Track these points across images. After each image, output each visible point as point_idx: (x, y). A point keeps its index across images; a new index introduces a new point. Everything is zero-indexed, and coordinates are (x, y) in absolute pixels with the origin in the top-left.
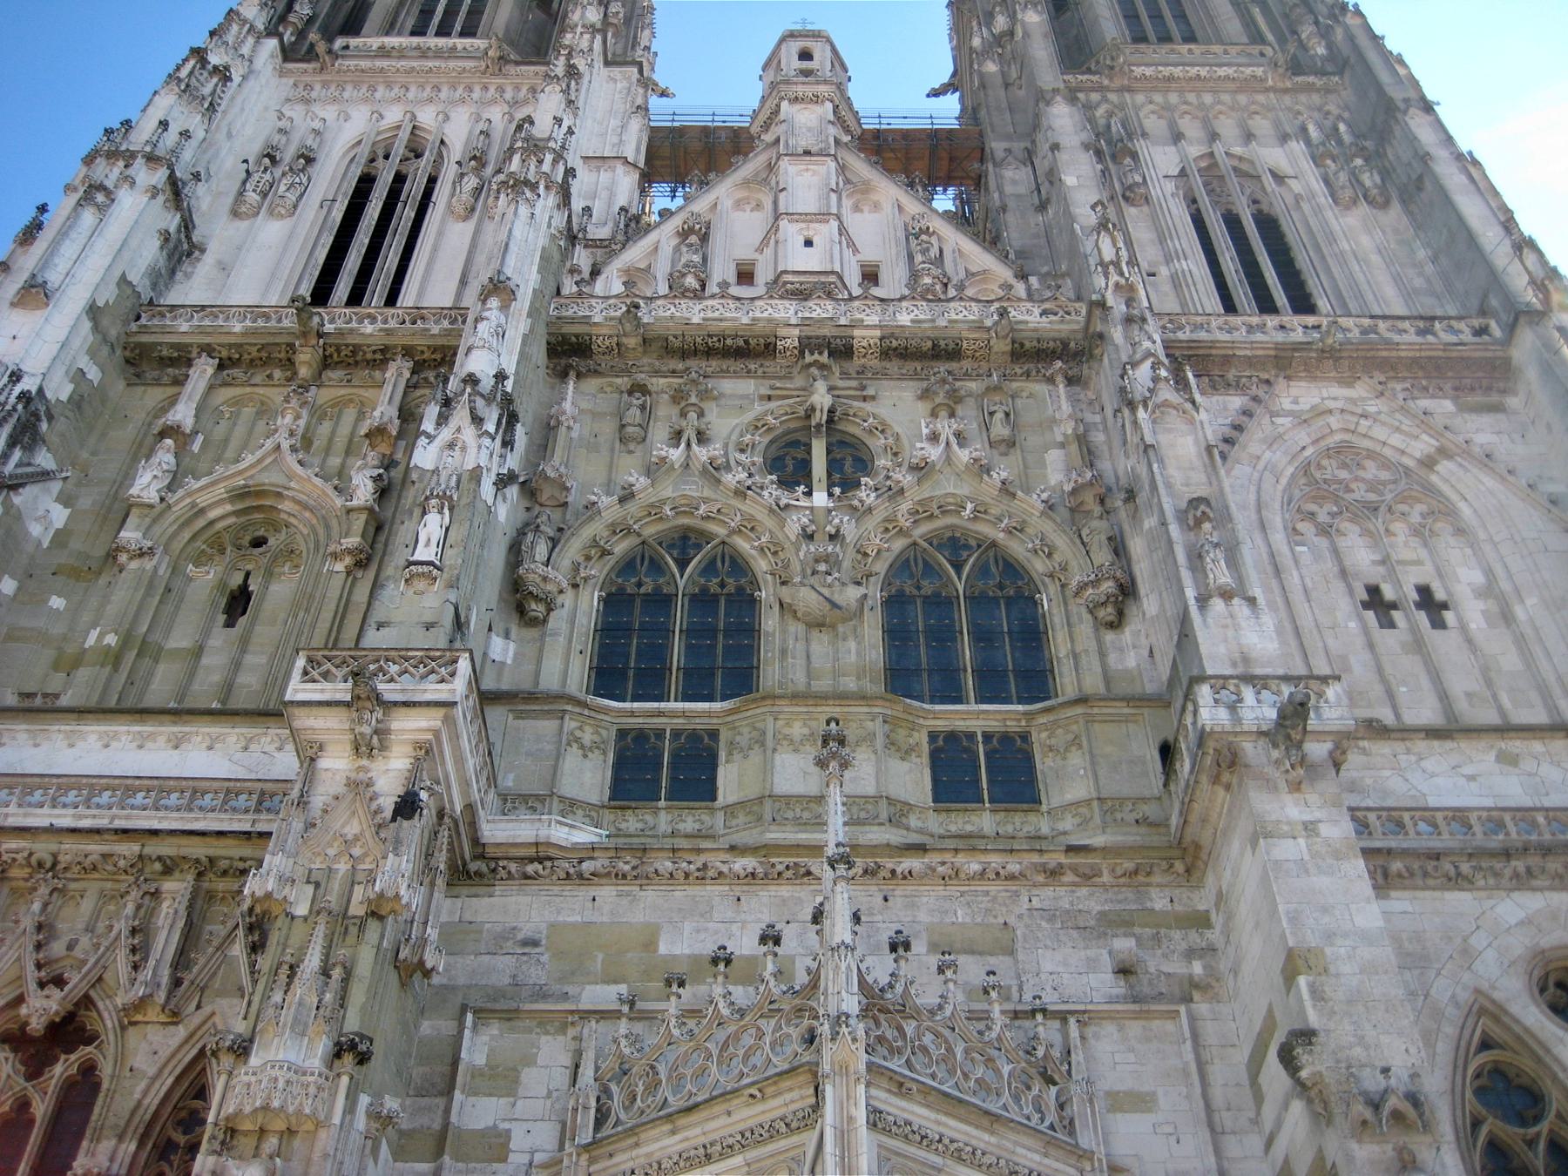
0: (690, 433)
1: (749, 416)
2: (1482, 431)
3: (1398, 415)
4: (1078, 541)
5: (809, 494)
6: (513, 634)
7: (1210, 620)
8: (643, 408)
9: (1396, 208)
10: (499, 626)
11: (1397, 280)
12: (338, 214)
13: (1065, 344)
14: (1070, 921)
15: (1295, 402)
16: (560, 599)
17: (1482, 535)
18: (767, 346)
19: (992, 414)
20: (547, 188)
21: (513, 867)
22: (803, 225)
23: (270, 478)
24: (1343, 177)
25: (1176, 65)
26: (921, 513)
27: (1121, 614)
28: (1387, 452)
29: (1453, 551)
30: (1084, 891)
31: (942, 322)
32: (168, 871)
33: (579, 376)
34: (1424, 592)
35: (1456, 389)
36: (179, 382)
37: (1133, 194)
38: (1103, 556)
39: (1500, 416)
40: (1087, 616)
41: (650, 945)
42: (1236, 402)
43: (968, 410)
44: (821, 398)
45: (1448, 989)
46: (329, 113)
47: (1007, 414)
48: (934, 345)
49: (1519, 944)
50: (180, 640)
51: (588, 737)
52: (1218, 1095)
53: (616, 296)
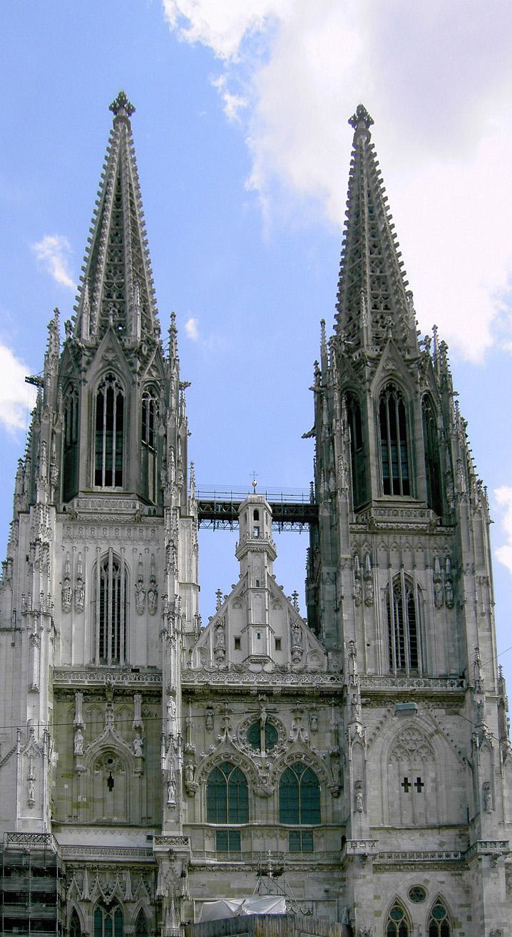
2: (449, 724)
3: (428, 717)
9: (455, 610)
12: (98, 612)
13: (336, 692)
14: (317, 880)
19: (312, 719)
21: (198, 869)
23: (110, 742)
24: (441, 594)
25: (394, 523)
27: (339, 794)
28: (421, 730)
29: (430, 764)
30: (320, 873)
32: (123, 869)
34: (419, 779)
35: (448, 705)
36: (73, 700)
37: (368, 603)
39: (457, 717)
41: (229, 885)
42: (383, 711)
44: (264, 716)
45: (391, 895)
46: (79, 546)
50: (99, 796)
51: (210, 834)
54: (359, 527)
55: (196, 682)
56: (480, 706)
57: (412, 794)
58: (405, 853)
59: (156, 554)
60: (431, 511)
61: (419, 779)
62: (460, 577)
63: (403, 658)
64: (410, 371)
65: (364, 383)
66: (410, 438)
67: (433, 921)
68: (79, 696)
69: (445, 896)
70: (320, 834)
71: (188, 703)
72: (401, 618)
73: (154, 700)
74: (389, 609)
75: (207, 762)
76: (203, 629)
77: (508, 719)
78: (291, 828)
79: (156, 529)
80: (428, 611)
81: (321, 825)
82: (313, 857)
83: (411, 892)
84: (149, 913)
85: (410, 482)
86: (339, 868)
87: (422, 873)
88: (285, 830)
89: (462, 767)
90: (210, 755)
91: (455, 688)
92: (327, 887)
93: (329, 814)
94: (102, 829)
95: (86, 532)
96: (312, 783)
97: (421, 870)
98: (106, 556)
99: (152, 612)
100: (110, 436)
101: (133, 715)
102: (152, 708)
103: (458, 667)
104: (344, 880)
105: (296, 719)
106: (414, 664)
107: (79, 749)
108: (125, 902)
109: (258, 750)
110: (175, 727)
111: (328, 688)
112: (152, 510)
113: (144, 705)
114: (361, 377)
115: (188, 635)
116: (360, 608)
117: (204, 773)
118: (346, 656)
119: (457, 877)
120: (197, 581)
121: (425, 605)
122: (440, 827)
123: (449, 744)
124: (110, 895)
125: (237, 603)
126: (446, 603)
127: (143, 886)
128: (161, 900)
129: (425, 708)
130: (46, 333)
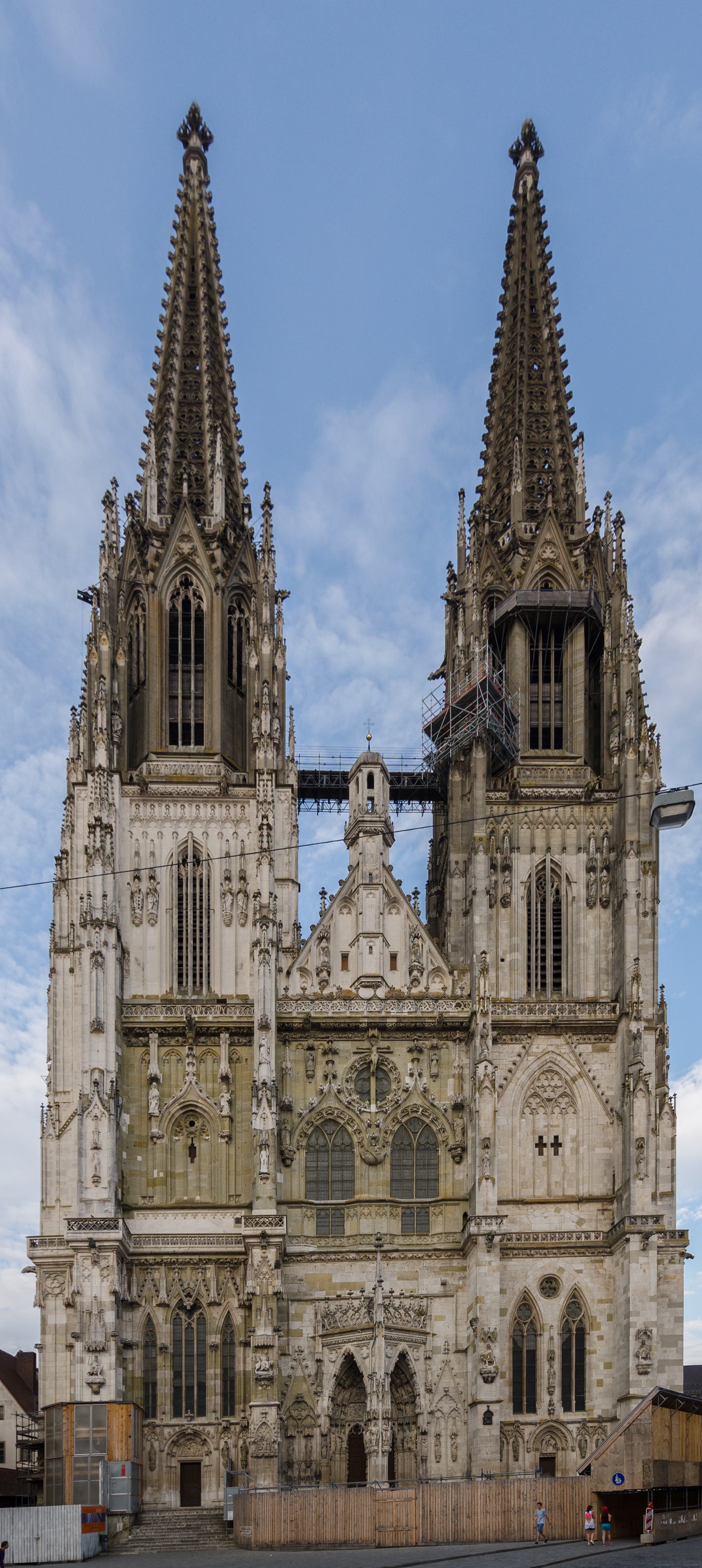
1: (349, 1063)
3: (571, 1055)
8: (313, 1060)
11: (597, 963)
15: (537, 1048)
17: (581, 1115)
21: (294, 1258)
23: (191, 1097)
26: (405, 1112)
27: (461, 1158)
32: (206, 1263)
33: (289, 1042)
36: (146, 1045)
37: (506, 902)
39: (605, 1054)
40: (451, 1160)
41: (330, 1280)
42: (518, 1048)
43: (424, 1057)
45: (518, 1287)
46: (153, 831)
49: (539, 1274)
51: (309, 1213)
52: (459, 1318)
54: (498, 794)
55: (296, 1012)
56: (636, 1037)
57: (548, 1157)
58: (537, 1233)
59: (247, 842)
60: (589, 769)
61: (556, 1138)
62: (620, 862)
63: (543, 977)
64: (573, 559)
65: (512, 581)
66: (567, 663)
67: (567, 1321)
68: (154, 1036)
69: (583, 1289)
70: (437, 1210)
71: (284, 1043)
72: (543, 923)
73: (244, 1040)
74: (529, 910)
75: (306, 1119)
76: (305, 942)
77: (668, 1057)
78: (404, 1203)
79: (246, 806)
80: (578, 913)
81: (439, 1198)
82: (429, 1240)
83: (541, 1284)
84: (238, 1317)
85: (564, 729)
86: (458, 1255)
87: (556, 1259)
88: (398, 1207)
89: (609, 1121)
91: (606, 1016)
92: (444, 1279)
93: (449, 1185)
94: (182, 1211)
95: (160, 810)
96: (430, 1147)
97: (555, 1255)
98: (184, 846)
99: (242, 921)
100: (186, 672)
101: (219, 1062)
102: (242, 1051)
103: (610, 988)
104: (464, 1269)
105: (413, 1061)
106: (557, 985)
107: (154, 1108)
108: (210, 1304)
109: (367, 1102)
110: (266, 1073)
111: (452, 1017)
112: (241, 778)
113: (232, 1048)
114: (509, 572)
115: (286, 951)
116: (494, 910)
117: (304, 1134)
118: (477, 973)
119: (598, 1264)
120: (297, 877)
121: (574, 905)
122: (581, 1200)
123: (595, 1090)
124: (191, 1297)
125: (345, 907)
126: (601, 900)
127: (230, 1285)
128: (251, 1300)
129: (568, 1043)
130: (99, 513)
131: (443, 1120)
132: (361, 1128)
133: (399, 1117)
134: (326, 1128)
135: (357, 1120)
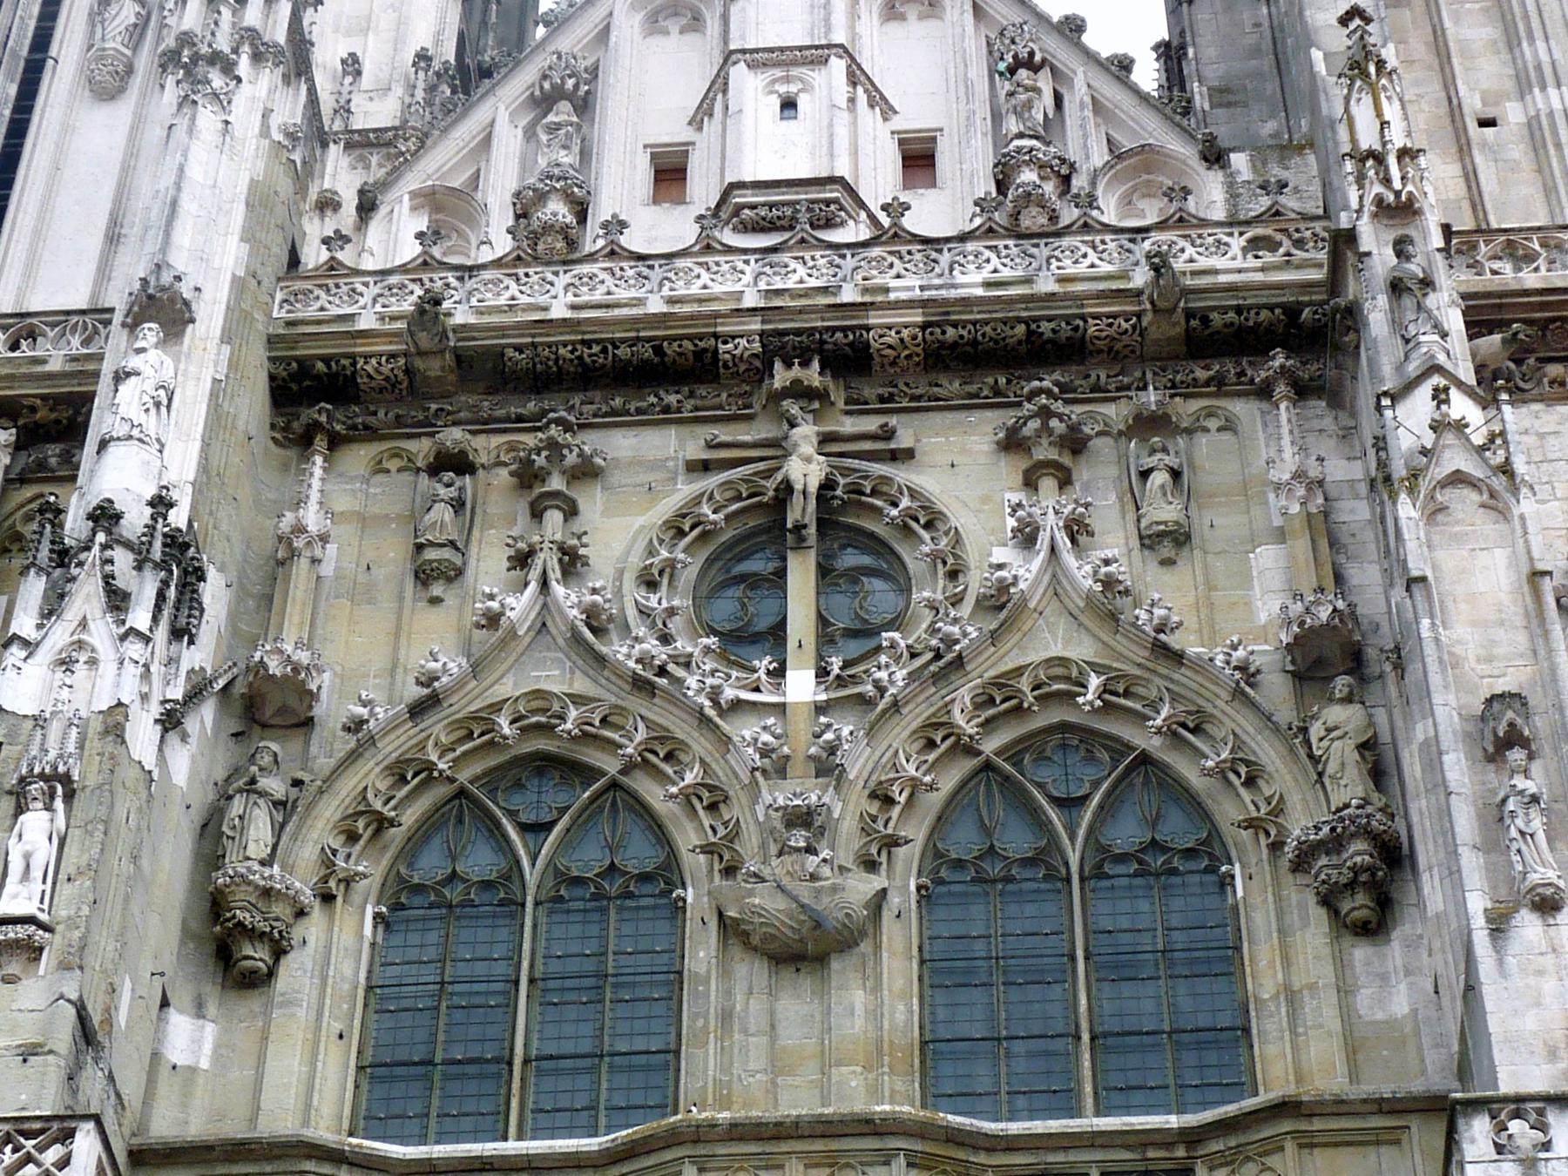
0: (548, 559)
4: (1302, 752)
5: (779, 673)
6: (212, 1009)
7: (1510, 961)
8: (458, 505)
10: (182, 995)
13: (1292, 311)
16: (297, 933)
18: (699, 354)
19: (1145, 475)
20: (257, 57)
22: (778, 73)
31: (1046, 285)
33: (336, 442)
38: (1350, 787)
40: (1319, 915)
47: (1176, 474)
48: (1030, 333)
53: (403, 269)
75: (391, 748)
90: (417, 710)
115: (361, 143)
131: (1233, 720)
132: (722, 776)
133: (959, 719)
134: (516, 802)
135: (700, 744)
